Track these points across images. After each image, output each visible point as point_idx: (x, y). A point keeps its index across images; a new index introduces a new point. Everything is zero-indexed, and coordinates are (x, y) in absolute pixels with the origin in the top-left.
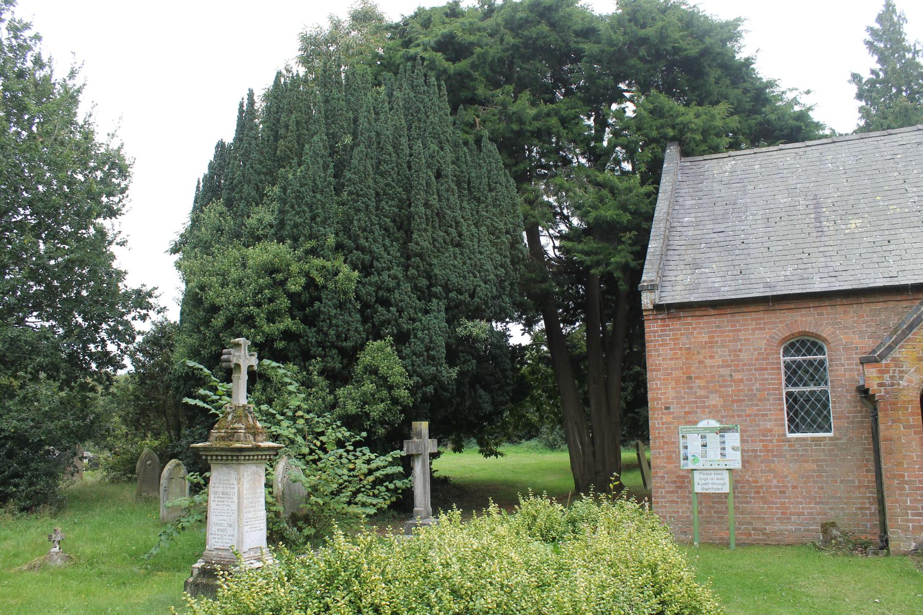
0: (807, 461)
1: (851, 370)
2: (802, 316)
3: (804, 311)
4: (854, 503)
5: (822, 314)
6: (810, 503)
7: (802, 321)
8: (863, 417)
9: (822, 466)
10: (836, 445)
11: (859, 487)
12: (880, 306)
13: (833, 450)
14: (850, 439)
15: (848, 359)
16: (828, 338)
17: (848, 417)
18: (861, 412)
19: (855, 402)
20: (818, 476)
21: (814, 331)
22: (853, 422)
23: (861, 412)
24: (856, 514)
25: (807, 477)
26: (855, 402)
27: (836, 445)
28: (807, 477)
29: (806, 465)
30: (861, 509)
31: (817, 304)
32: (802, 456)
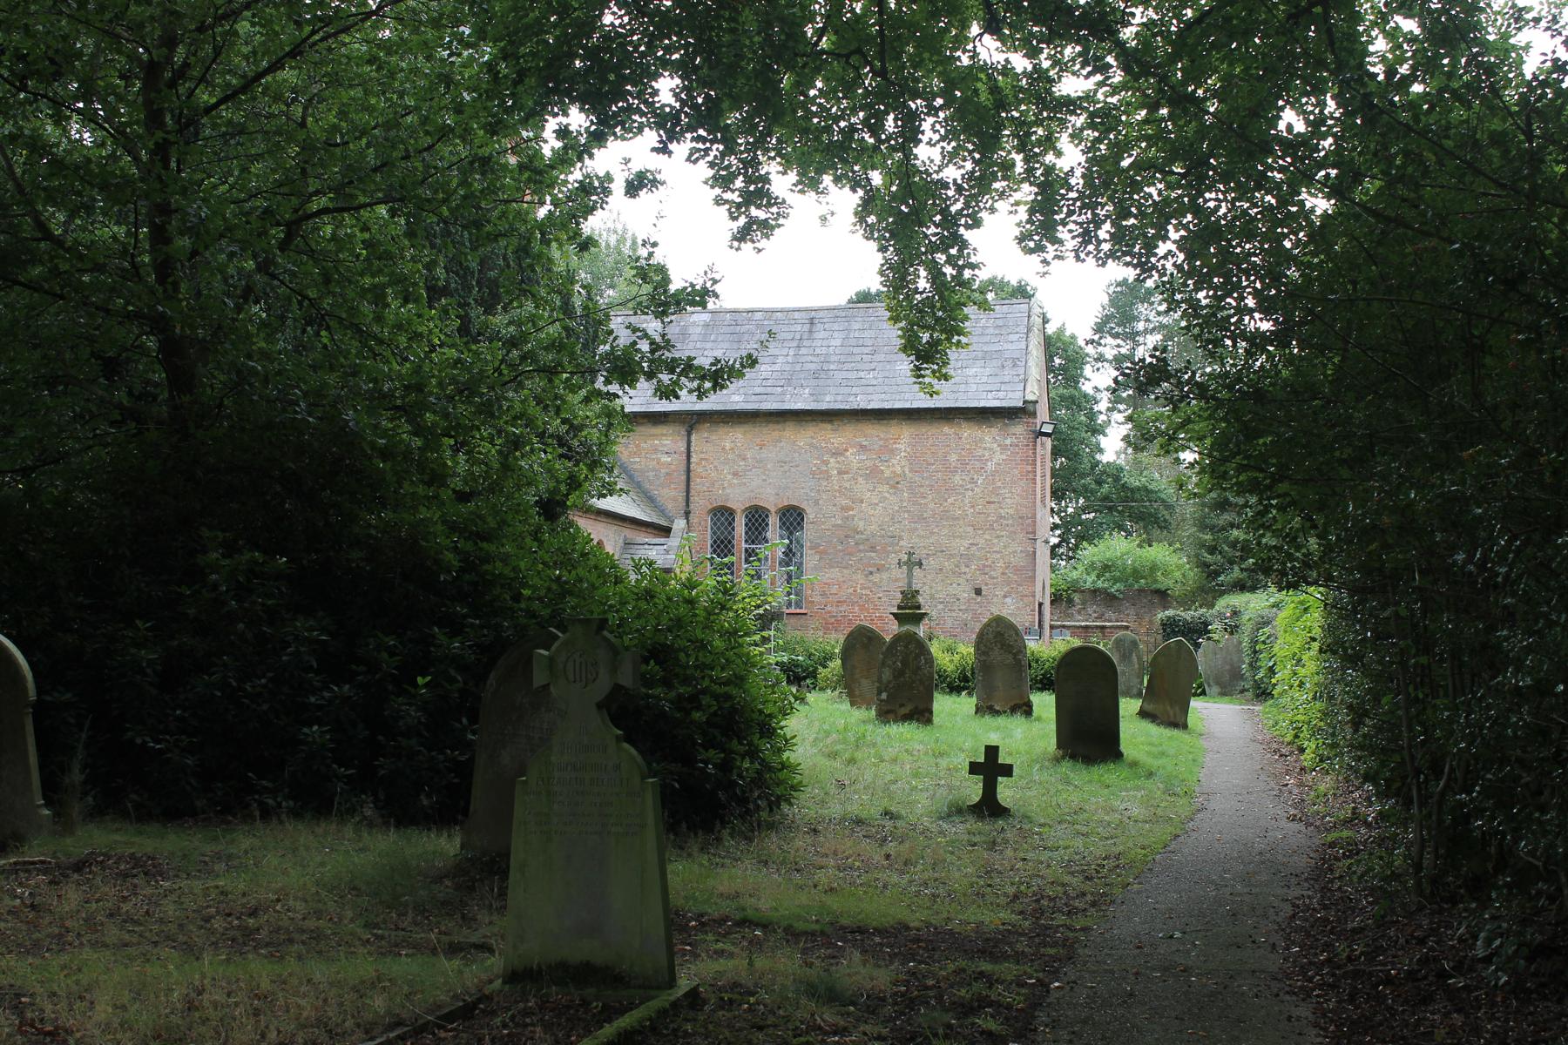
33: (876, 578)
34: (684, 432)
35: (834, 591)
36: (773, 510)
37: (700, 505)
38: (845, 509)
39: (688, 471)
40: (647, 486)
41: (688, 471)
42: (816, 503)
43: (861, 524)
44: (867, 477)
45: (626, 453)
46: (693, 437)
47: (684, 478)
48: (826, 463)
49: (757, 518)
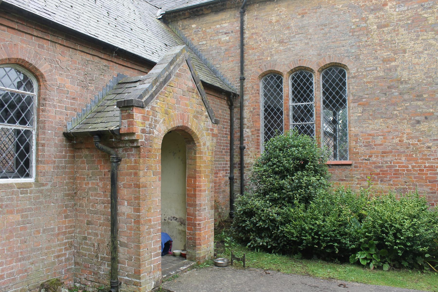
0: (11, 212)
1: (61, 113)
2: (22, 41)
3: (26, 37)
4: (53, 252)
5: (42, 47)
6: (11, 262)
7: (22, 47)
8: (66, 162)
9: (27, 216)
10: (41, 192)
11: (58, 234)
12: (89, 57)
13: (38, 197)
14: (54, 185)
15: (60, 101)
16: (45, 75)
17: (55, 162)
18: (65, 157)
19: (61, 146)
20: (22, 229)
21: (33, 62)
22: (58, 167)
23: (65, 157)
24: (54, 263)
25: (11, 232)
26: (61, 146)
27: (41, 192)
28: (11, 232)
29: (11, 217)
30: (58, 256)
31: (40, 34)
32: (7, 206)
33: (424, 126)
34: (238, 14)
35: (378, 142)
36: (315, 68)
37: (253, 72)
38: (386, 61)
39: (242, 45)
40: (211, 62)
41: (242, 45)
42: (357, 58)
43: (405, 74)
44: (409, 27)
45: (196, 39)
46: (246, 18)
47: (239, 51)
48: (365, 20)
49: (302, 78)
